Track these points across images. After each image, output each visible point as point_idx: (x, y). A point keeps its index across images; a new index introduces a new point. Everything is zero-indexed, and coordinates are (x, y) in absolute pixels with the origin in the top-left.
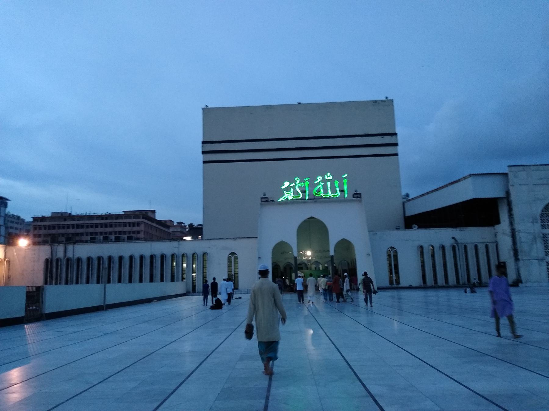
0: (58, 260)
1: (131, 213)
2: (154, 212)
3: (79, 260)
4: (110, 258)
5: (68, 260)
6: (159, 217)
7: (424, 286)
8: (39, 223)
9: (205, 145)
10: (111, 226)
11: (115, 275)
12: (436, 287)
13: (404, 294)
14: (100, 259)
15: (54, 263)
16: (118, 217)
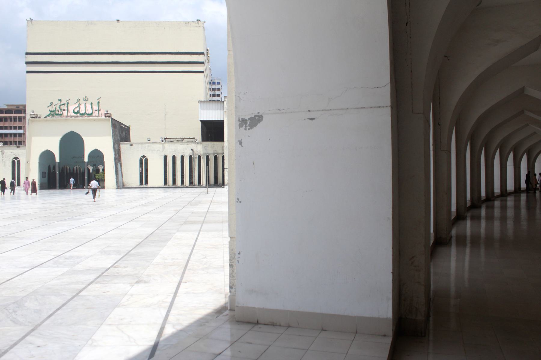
1: (15, 108)
9: (29, 56)
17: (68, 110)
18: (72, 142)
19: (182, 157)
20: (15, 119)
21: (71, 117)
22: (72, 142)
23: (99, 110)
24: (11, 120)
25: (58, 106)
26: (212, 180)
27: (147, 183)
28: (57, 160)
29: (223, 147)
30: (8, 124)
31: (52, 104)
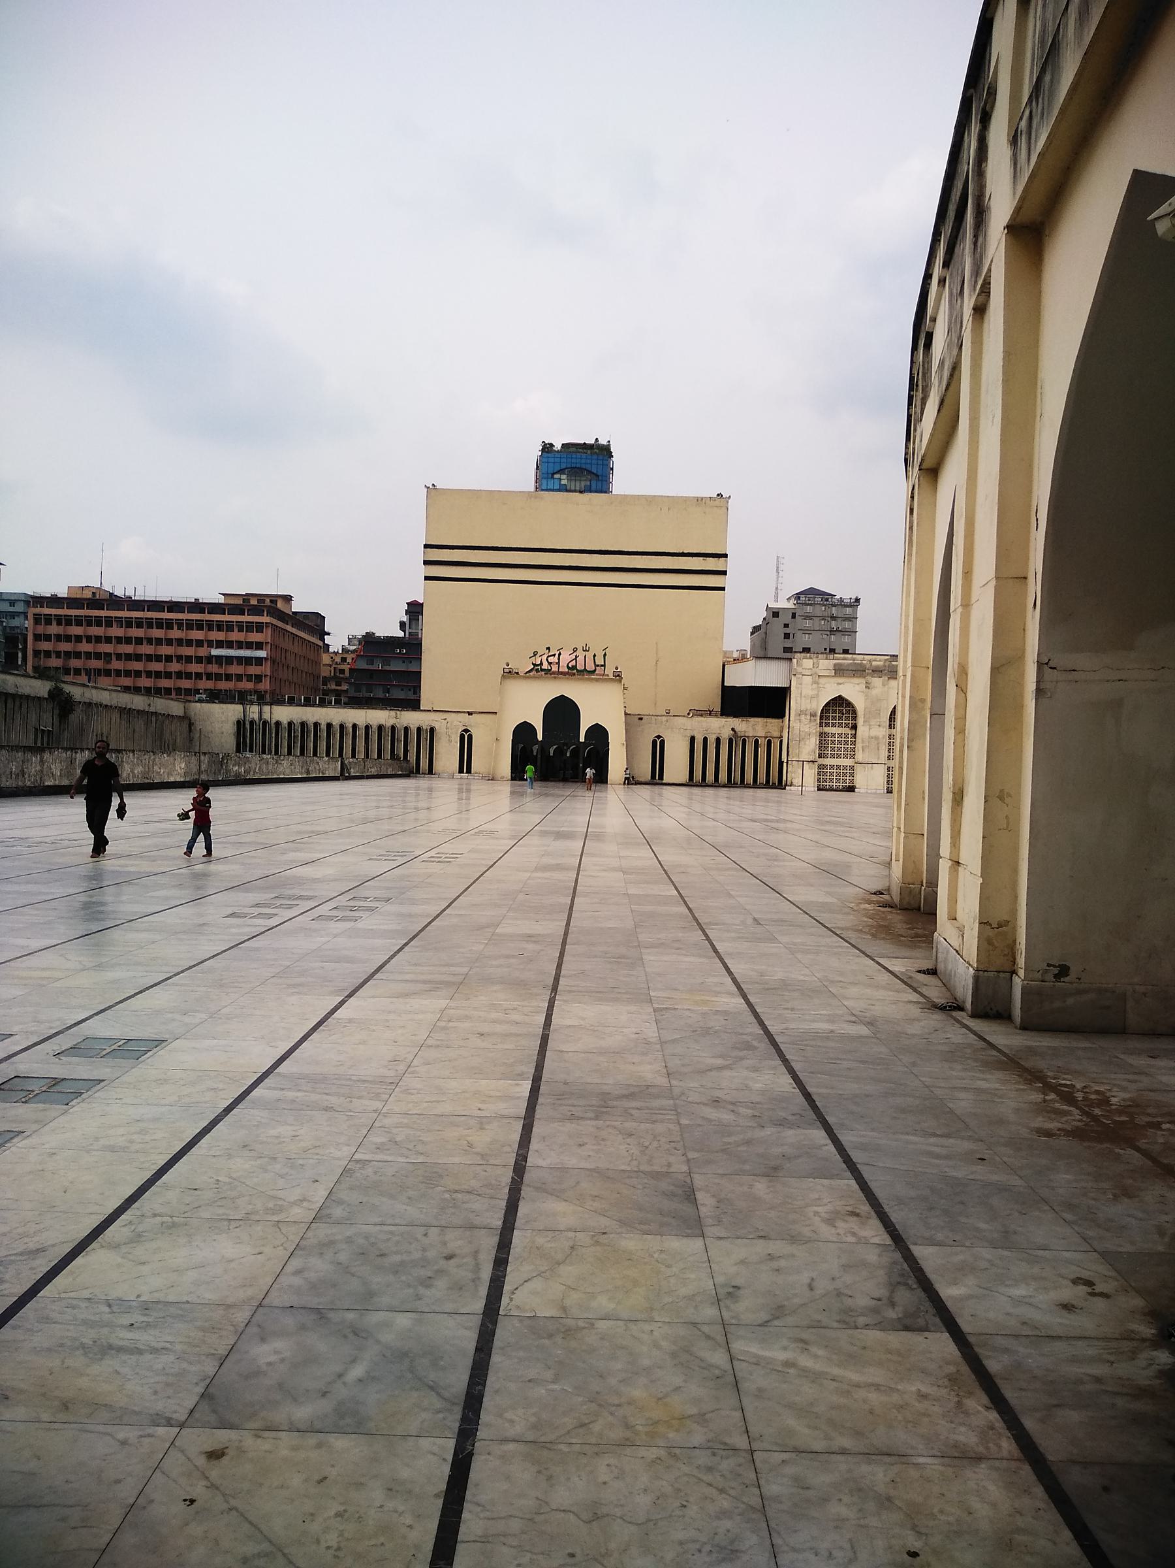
0: (252, 723)
1: (240, 601)
2: (288, 599)
3: (278, 724)
4: (316, 724)
5: (265, 723)
6: (297, 606)
7: (690, 783)
8: (46, 611)
10: (200, 627)
11: (322, 746)
12: (703, 784)
13: (667, 790)
14: (303, 724)
15: (248, 726)
16: (215, 608)
17: (558, 663)
18: (562, 712)
19: (718, 740)
20: (249, 627)
21: (562, 673)
22: (562, 712)
23: (604, 666)
24: (241, 630)
25: (544, 657)
26: (762, 778)
27: (661, 777)
28: (540, 737)
29: (782, 728)
30: (235, 636)
31: (535, 654)
